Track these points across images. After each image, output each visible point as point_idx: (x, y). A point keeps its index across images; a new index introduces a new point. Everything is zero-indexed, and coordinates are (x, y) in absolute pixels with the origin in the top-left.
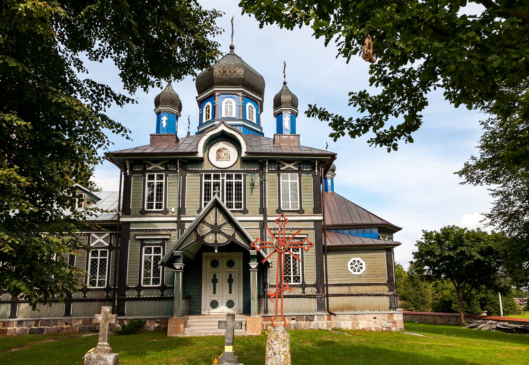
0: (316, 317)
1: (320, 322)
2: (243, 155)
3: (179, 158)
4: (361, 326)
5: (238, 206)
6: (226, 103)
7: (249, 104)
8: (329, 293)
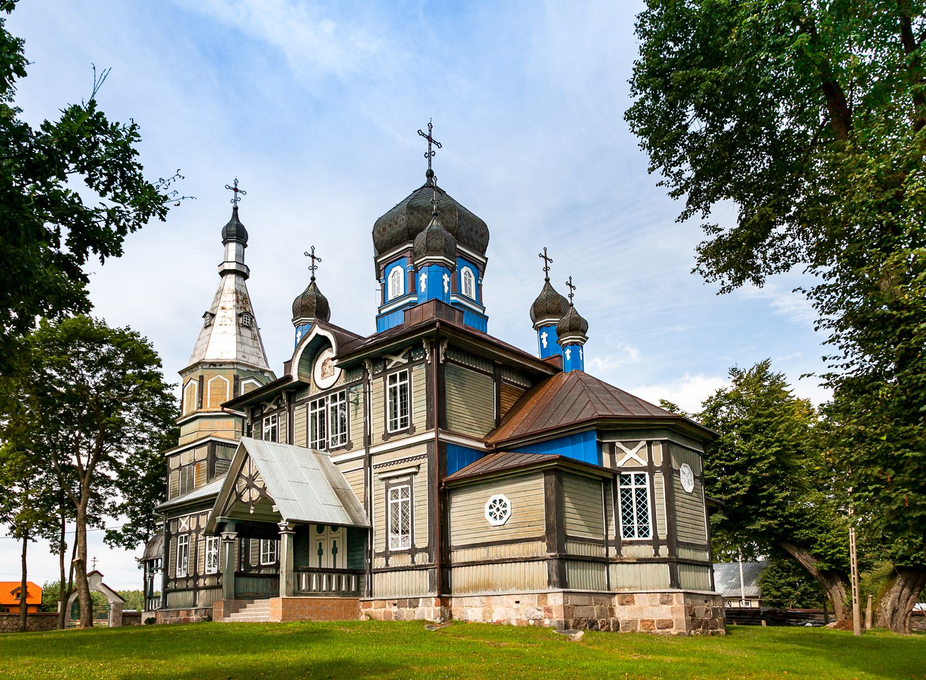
1: (426, 609)
4: (496, 618)
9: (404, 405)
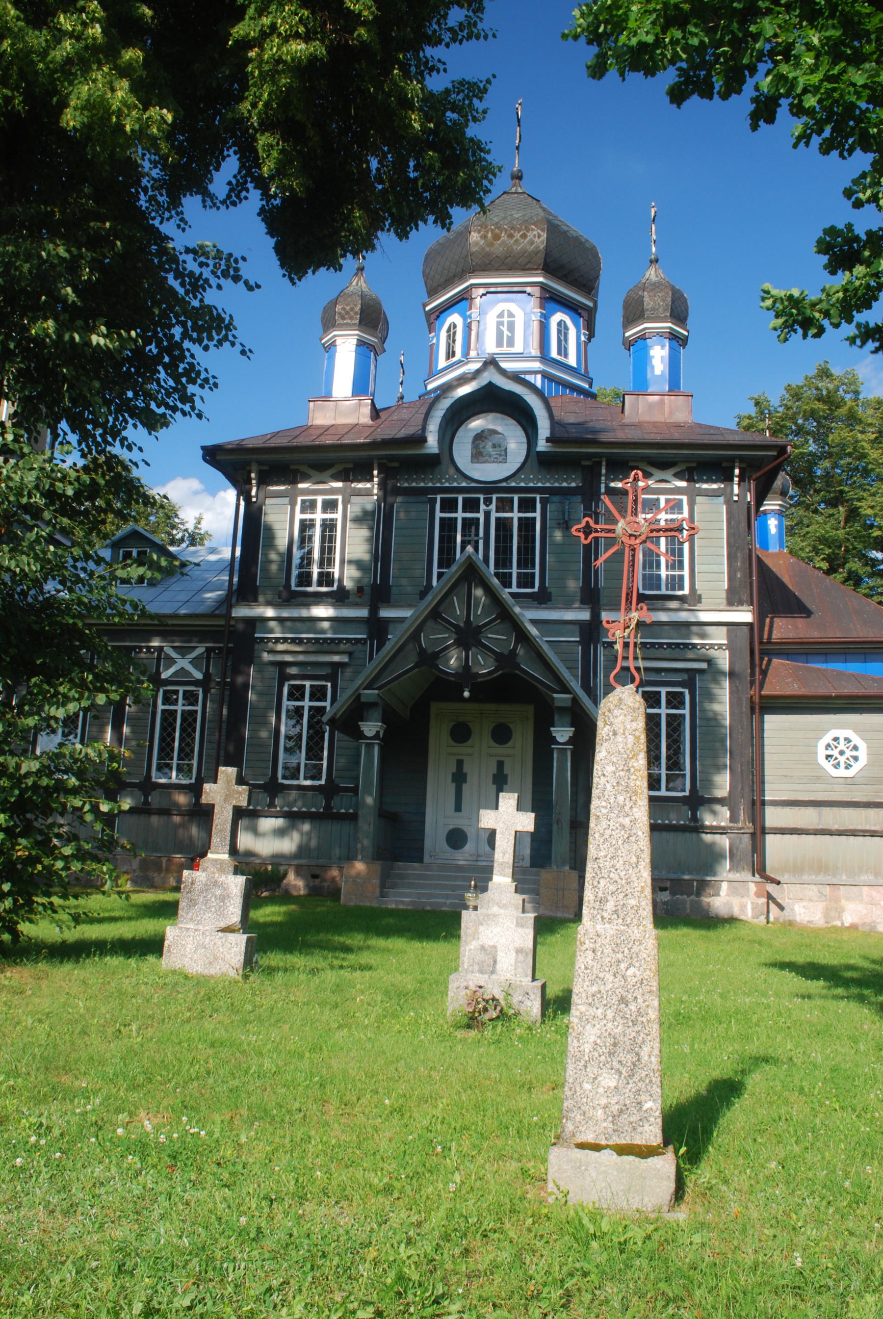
2: (542, 445)
3: (380, 458)
5: (526, 580)
6: (501, 315)
7: (559, 316)
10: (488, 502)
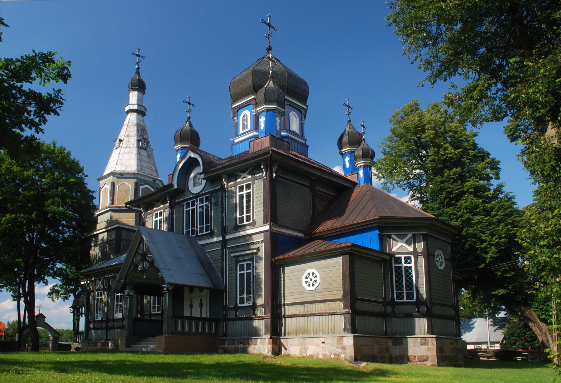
0: (259, 340)
1: (262, 346)
4: (309, 353)
6: (244, 117)
8: (287, 314)
9: (248, 207)
10: (197, 201)
